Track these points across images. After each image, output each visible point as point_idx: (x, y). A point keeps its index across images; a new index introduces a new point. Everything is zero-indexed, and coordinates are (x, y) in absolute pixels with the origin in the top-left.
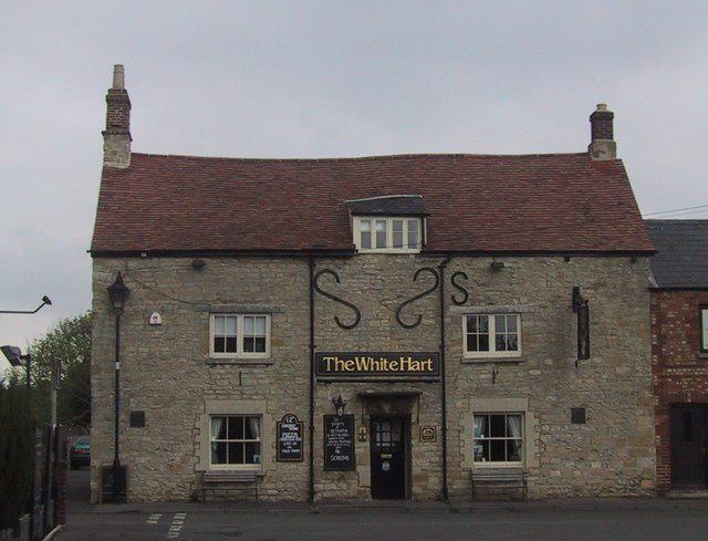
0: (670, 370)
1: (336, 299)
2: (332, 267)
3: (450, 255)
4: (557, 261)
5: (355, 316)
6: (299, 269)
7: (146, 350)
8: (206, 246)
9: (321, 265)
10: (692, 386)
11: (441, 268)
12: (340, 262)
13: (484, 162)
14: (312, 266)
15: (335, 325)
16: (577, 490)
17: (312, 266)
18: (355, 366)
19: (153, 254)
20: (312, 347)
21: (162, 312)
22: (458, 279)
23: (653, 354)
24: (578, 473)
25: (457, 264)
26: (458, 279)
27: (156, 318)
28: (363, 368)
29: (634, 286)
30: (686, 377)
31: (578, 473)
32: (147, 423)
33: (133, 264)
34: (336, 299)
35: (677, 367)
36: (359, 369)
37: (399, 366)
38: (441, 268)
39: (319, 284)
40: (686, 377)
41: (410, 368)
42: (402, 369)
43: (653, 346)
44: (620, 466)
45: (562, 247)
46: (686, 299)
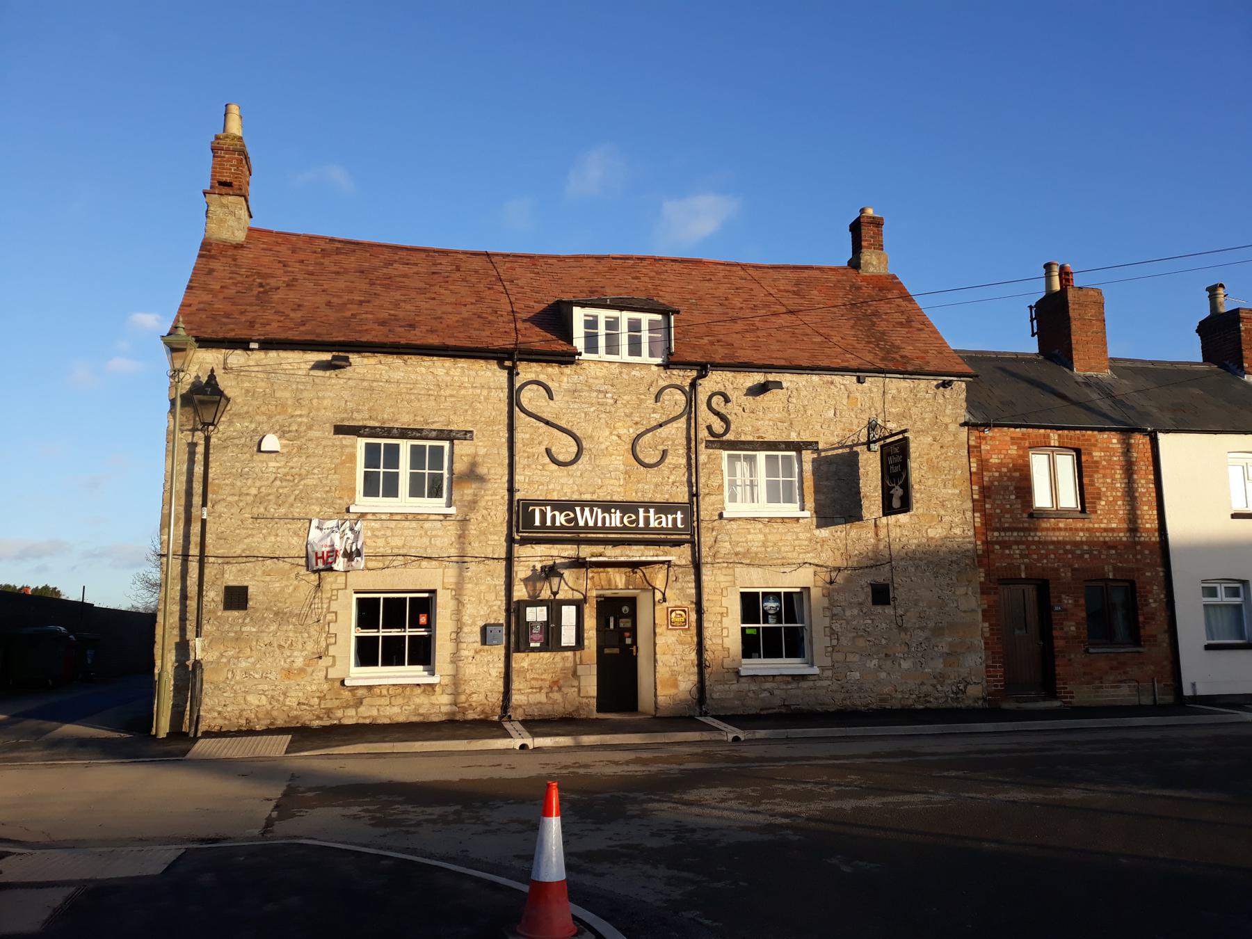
0: (996, 534)
1: (547, 423)
2: (542, 378)
3: (703, 369)
4: (850, 380)
5: (575, 449)
6: (492, 375)
7: (254, 491)
8: (353, 337)
9: (528, 372)
10: (1027, 556)
11: (693, 385)
12: (553, 370)
13: (728, 268)
14: (512, 374)
15: (547, 460)
16: (882, 700)
17: (512, 374)
18: (575, 518)
19: (268, 345)
20: (511, 490)
21: (283, 433)
22: (717, 402)
23: (974, 511)
24: (883, 675)
25: (714, 381)
26: (717, 402)
27: (271, 442)
28: (586, 522)
29: (947, 420)
30: (1017, 543)
31: (883, 675)
32: (250, 603)
33: (237, 358)
34: (547, 423)
35: (1005, 530)
36: (581, 523)
37: (637, 520)
38: (693, 385)
39: (525, 401)
40: (1017, 543)
41: (653, 524)
42: (641, 525)
43: (973, 501)
44: (939, 665)
45: (854, 364)
46: (1012, 438)
